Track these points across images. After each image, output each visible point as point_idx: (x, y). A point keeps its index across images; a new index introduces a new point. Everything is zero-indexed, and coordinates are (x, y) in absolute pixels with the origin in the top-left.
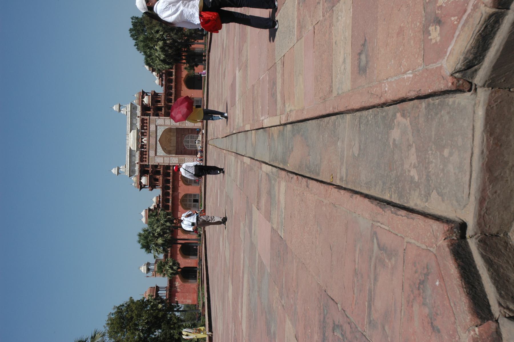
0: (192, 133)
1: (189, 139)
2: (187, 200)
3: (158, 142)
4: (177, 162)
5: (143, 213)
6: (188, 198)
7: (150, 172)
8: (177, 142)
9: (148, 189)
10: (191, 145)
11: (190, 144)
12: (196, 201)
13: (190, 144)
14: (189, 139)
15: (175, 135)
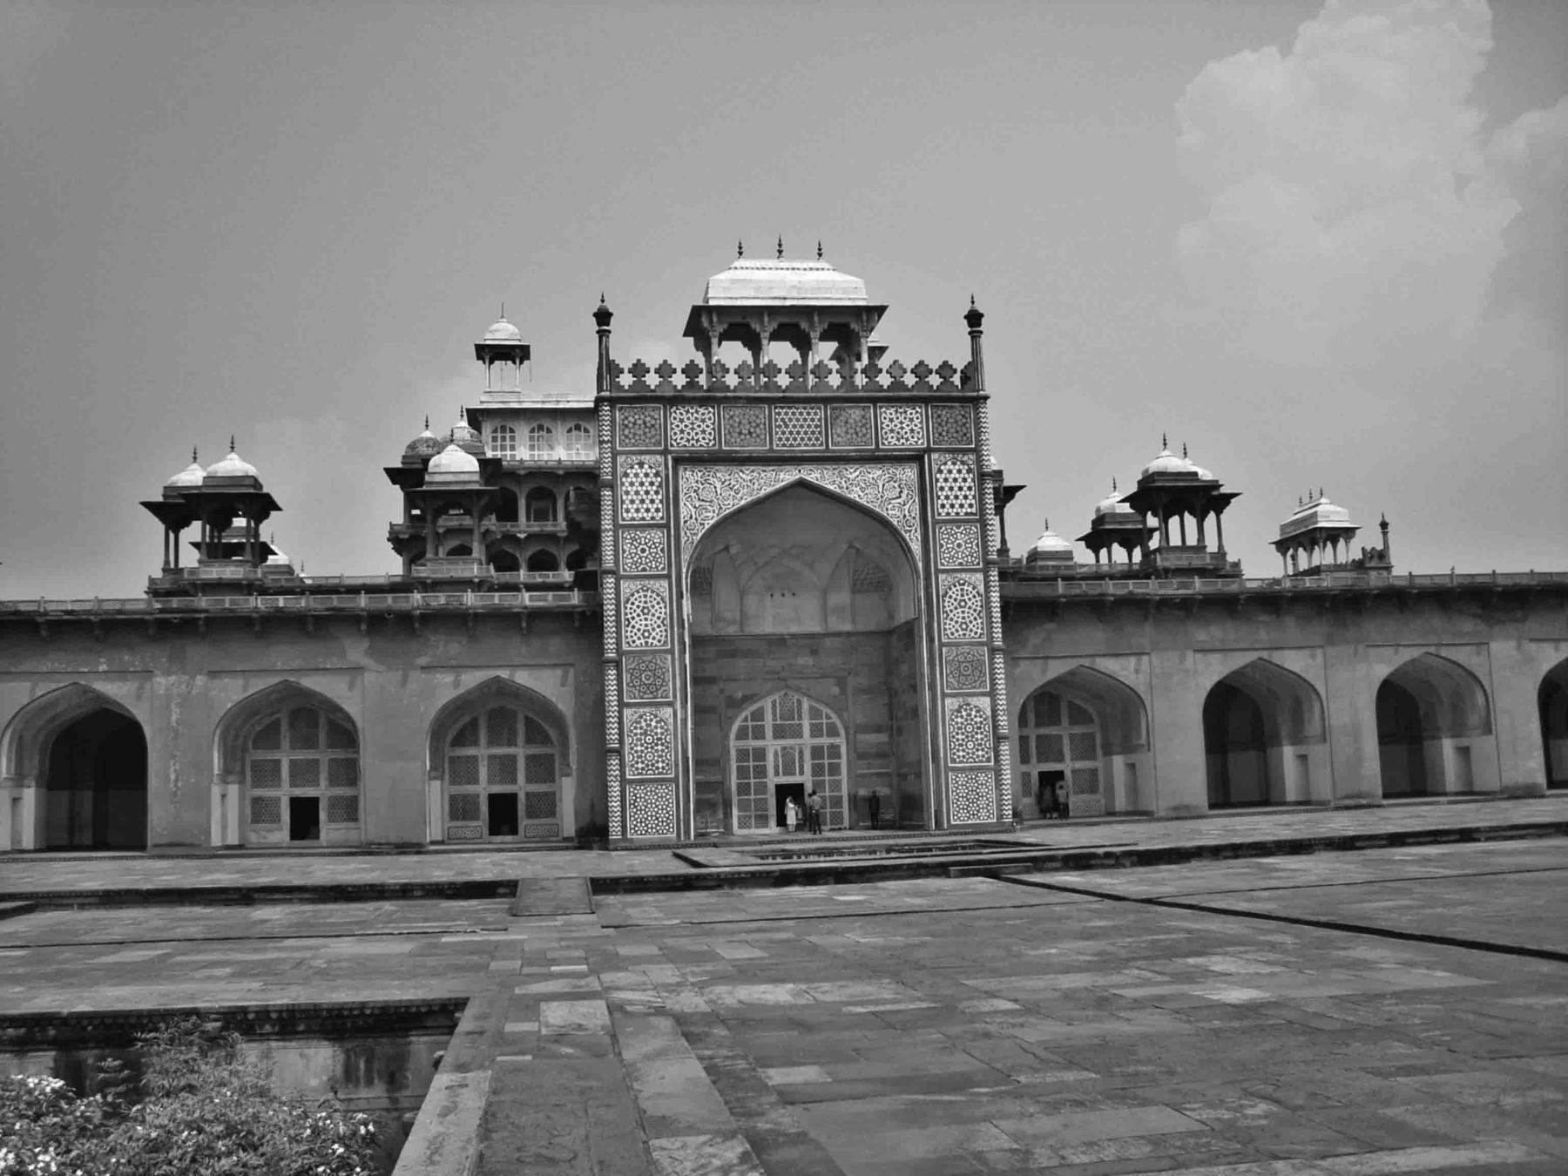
0: (859, 755)
1: (807, 740)
2: (310, 743)
3: (788, 476)
4: (634, 639)
5: (233, 465)
6: (324, 756)
7: (508, 527)
8: (778, 642)
9: (399, 519)
10: (760, 754)
11: (772, 746)
12: (304, 819)
13: (772, 746)
14: (807, 740)
15: (836, 625)
